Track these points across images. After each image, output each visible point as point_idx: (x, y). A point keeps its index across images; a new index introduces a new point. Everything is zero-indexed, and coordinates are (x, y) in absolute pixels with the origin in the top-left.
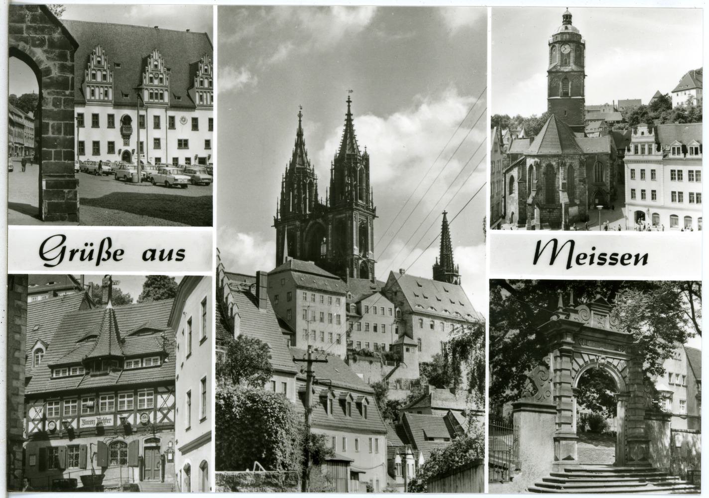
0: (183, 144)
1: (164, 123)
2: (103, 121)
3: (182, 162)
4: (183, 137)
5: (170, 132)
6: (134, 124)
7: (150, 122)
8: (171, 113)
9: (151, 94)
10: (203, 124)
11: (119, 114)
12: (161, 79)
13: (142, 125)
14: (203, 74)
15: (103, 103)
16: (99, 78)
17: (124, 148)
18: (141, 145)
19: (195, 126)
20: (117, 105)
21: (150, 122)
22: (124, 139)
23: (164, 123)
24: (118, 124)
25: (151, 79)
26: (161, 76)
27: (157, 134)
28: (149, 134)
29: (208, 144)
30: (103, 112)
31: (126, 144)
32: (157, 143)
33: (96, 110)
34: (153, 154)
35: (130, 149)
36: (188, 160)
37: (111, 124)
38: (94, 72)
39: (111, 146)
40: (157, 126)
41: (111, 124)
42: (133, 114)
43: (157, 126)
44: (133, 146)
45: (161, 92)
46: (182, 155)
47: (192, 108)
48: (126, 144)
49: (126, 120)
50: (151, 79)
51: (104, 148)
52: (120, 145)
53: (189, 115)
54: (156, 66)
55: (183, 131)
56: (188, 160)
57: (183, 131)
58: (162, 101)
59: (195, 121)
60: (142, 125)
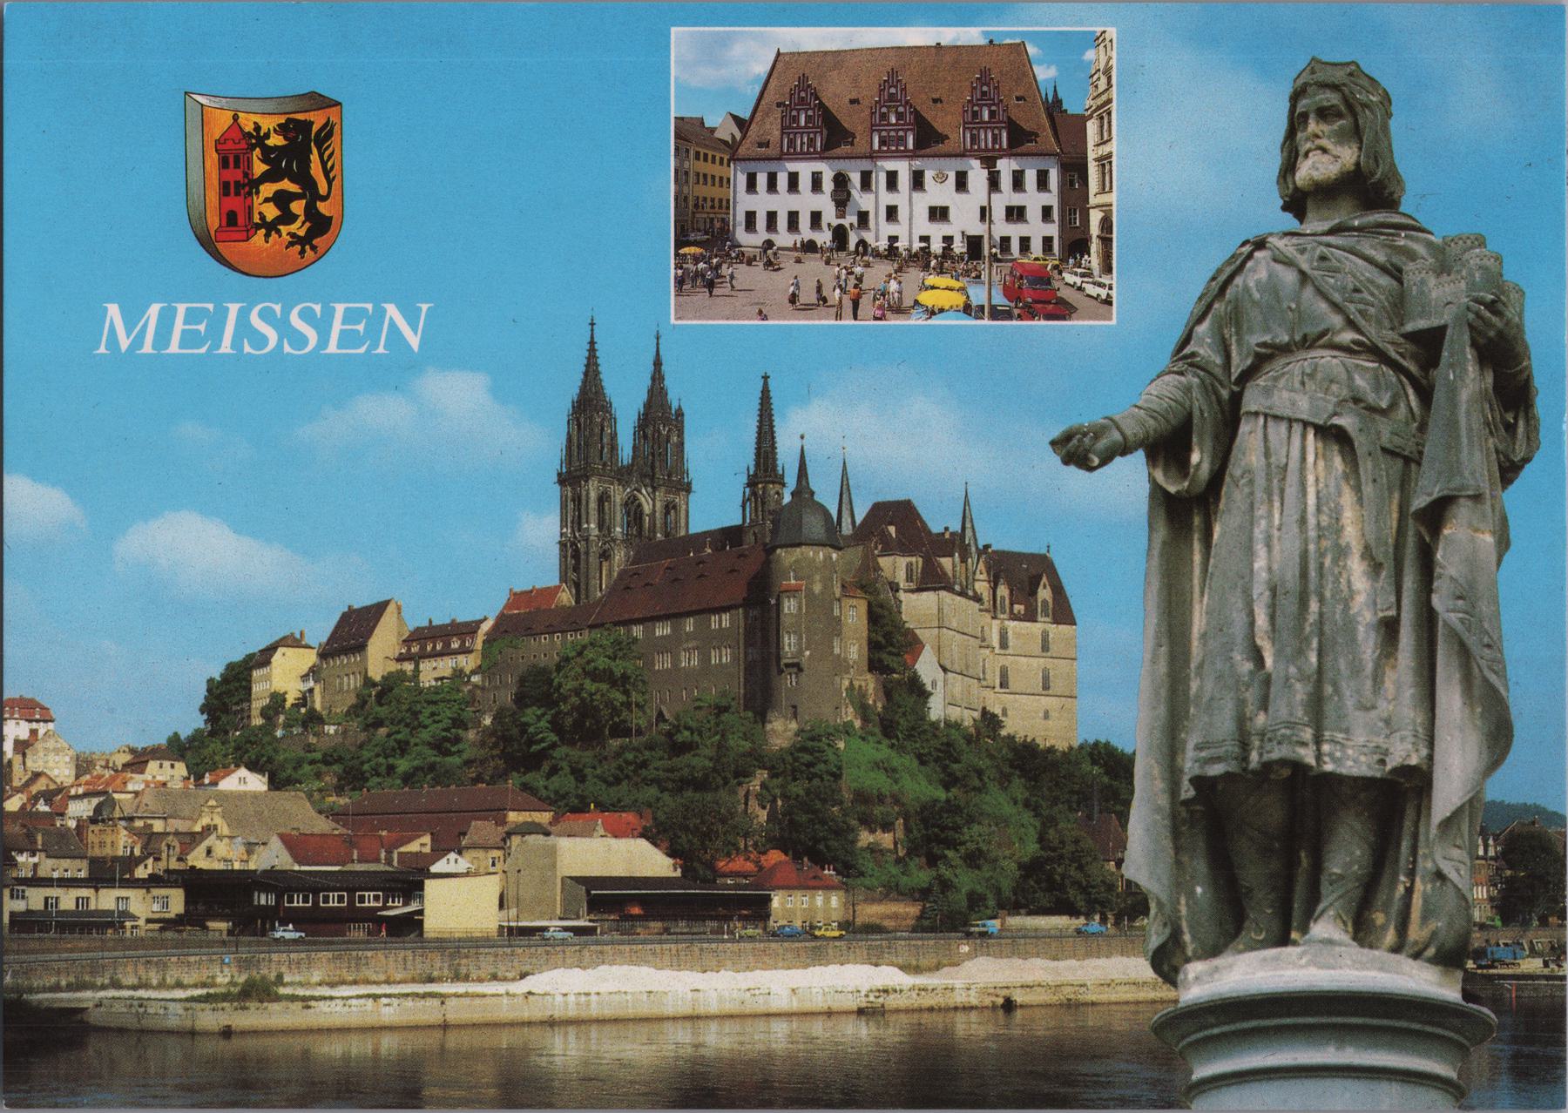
1: (904, 180)
2: (805, 182)
3: (937, 247)
5: (916, 195)
8: (918, 164)
17: (835, 222)
18: (863, 217)
23: (904, 180)
30: (805, 169)
31: (841, 215)
32: (892, 213)
33: (792, 166)
34: (888, 230)
35: (846, 222)
36: (948, 240)
37: (817, 184)
39: (816, 218)
46: (937, 232)
51: (804, 221)
52: (830, 216)
55: (939, 192)
56: (948, 240)
57: (939, 192)
60: (866, 183)
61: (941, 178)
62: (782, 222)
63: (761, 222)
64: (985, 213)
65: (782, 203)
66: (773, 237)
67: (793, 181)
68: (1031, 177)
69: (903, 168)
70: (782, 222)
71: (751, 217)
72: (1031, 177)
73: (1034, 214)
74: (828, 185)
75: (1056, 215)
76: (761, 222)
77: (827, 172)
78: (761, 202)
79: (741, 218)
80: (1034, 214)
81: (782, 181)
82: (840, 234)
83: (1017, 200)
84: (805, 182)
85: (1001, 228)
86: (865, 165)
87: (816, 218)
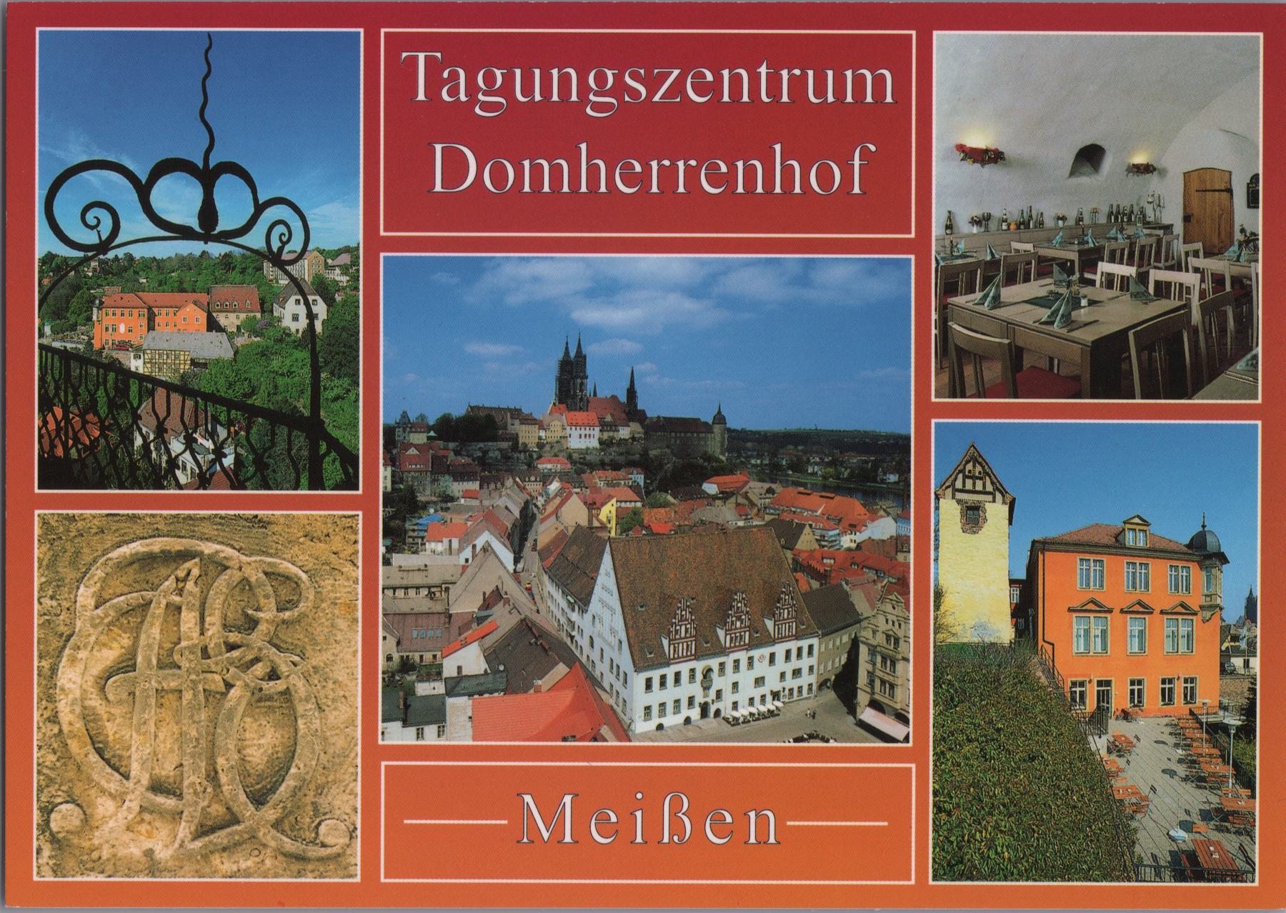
0: (759, 681)
7: (729, 667)
10: (780, 657)
15: (687, 659)
17: (702, 701)
18: (719, 693)
20: (697, 657)
21: (729, 667)
24: (699, 677)
27: (735, 678)
30: (684, 668)
31: (706, 696)
35: (709, 700)
39: (691, 701)
44: (712, 694)
48: (706, 696)
53: (766, 651)
55: (761, 668)
57: (761, 668)
59: (772, 656)
62: (670, 708)
63: (655, 711)
67: (677, 676)
69: (742, 656)
70: (670, 708)
71: (648, 709)
73: (805, 671)
76: (655, 711)
77: (700, 666)
79: (640, 712)
80: (805, 671)
85: (791, 683)
87: (691, 701)
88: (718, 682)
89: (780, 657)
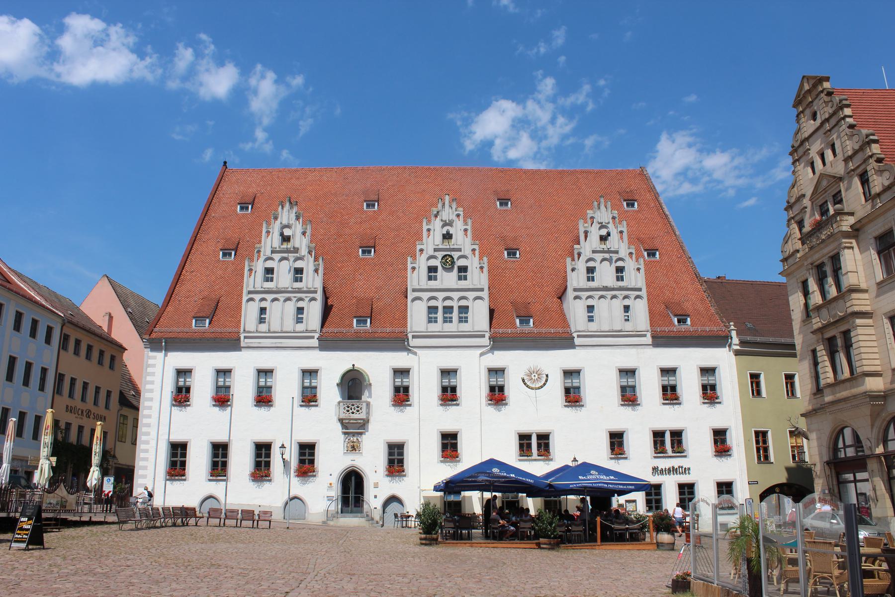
2: (286, 388)
4: (534, 427)
6: (380, 392)
8: (500, 358)
9: (432, 310)
10: (600, 386)
11: (334, 365)
12: (463, 269)
13: (401, 396)
14: (594, 252)
15: (281, 340)
16: (283, 277)
19: (572, 396)
20: (328, 343)
21: (425, 387)
22: (345, 433)
25: (432, 269)
26: (462, 262)
28: (420, 425)
29: (617, 441)
32: (449, 444)
37: (309, 398)
38: (269, 264)
40: (449, 395)
41: (309, 398)
42: (377, 366)
43: (449, 395)
45: (463, 303)
47: (565, 341)
48: (354, 448)
49: (353, 385)
50: (432, 269)
53: (553, 361)
54: (447, 236)
58: (464, 327)
60: (401, 396)
61: (535, 380)
62: (241, 460)
63: (198, 460)
64: (617, 441)
65: (244, 426)
66: (216, 488)
68: (689, 385)
69: (472, 368)
70: (241, 460)
72: (689, 385)
73: (698, 443)
74: (329, 392)
75: (737, 439)
76: (198, 460)
78: (200, 425)
80: (698, 443)
81: (243, 389)
82: (352, 485)
83: (668, 418)
84: (286, 388)
86: (400, 359)
88: (385, 422)
89: (600, 386)
